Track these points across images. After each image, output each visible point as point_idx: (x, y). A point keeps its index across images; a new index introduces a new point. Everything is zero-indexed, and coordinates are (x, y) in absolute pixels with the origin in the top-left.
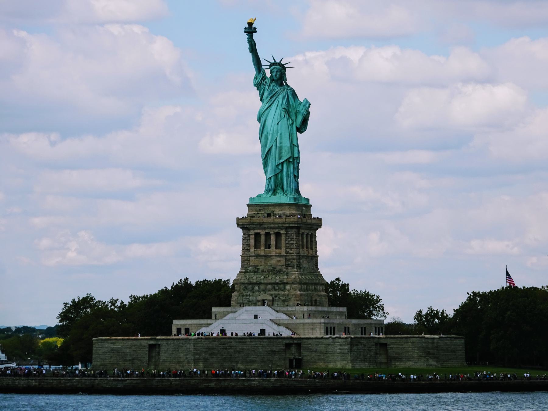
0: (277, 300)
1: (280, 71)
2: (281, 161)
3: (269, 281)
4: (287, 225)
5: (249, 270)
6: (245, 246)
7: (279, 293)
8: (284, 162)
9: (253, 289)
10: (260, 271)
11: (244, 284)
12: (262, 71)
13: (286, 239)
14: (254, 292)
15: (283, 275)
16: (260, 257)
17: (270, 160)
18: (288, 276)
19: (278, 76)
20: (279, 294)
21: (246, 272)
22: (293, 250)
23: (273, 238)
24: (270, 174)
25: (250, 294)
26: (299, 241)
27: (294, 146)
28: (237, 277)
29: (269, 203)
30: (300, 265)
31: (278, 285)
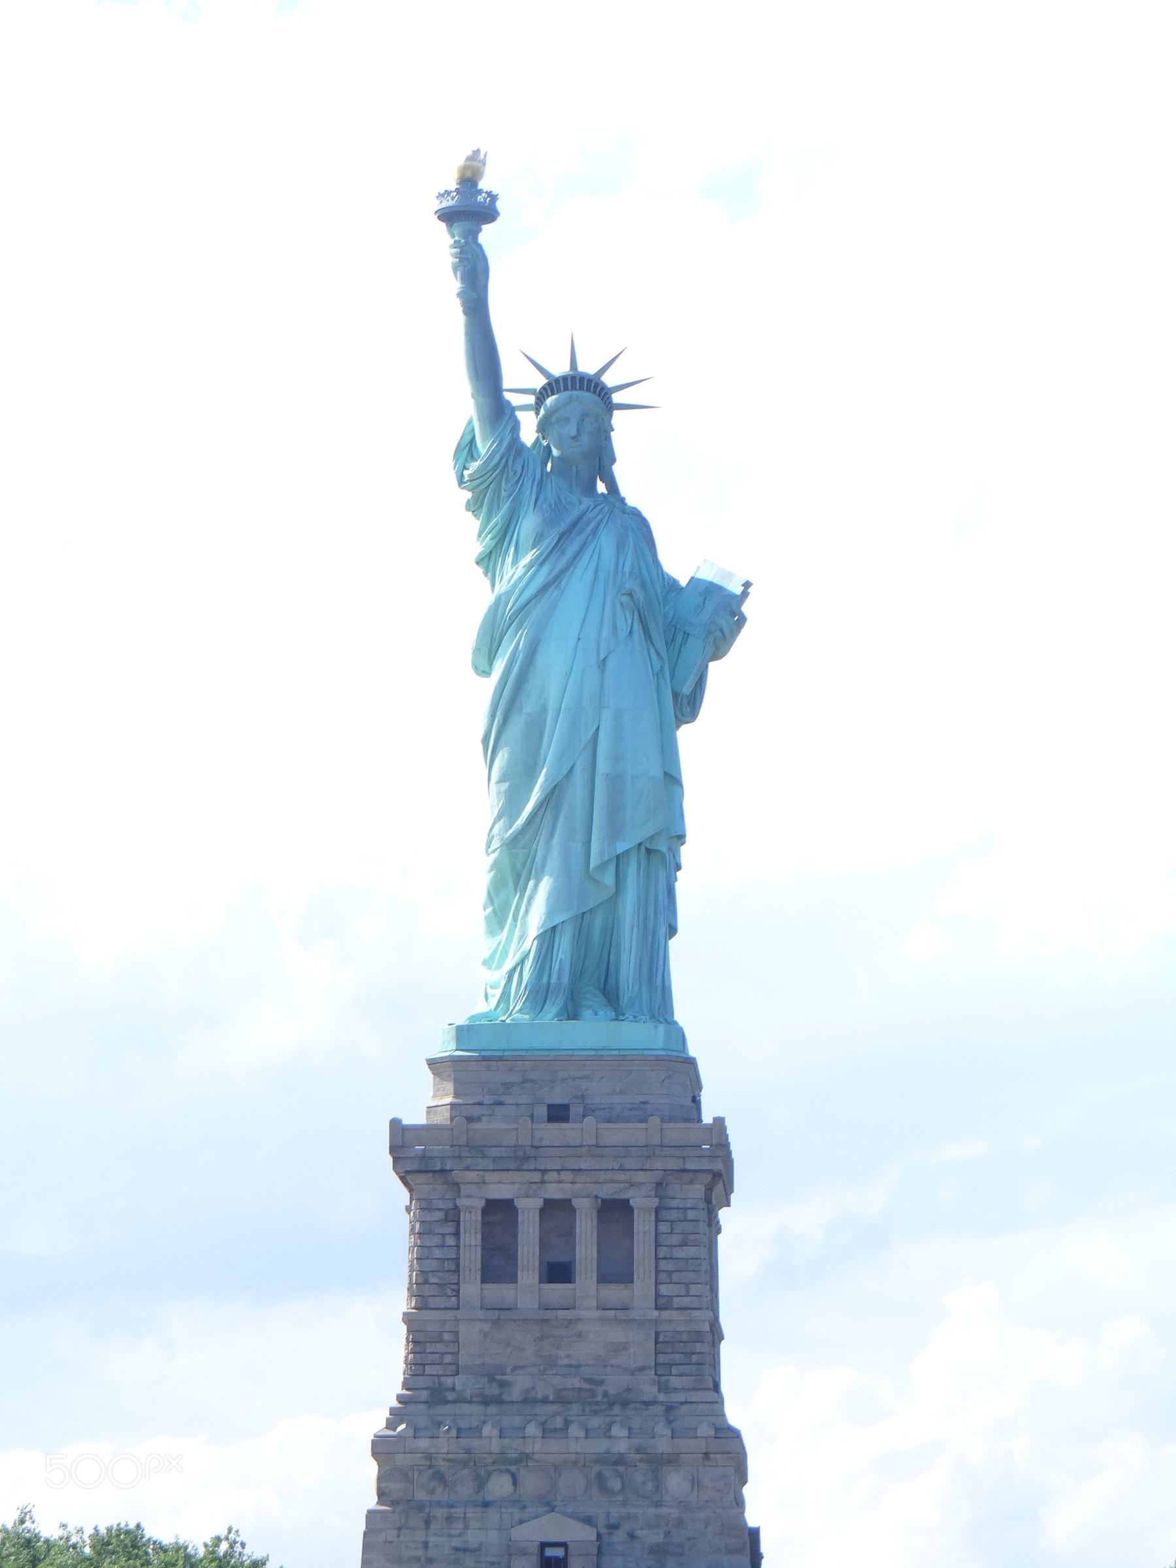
2: (621, 847)
4: (672, 1164)
5: (453, 1389)
8: (628, 851)
10: (516, 1394)
12: (508, 412)
14: (486, 1505)
19: (585, 439)
20: (629, 1517)
22: (694, 1289)
23: (586, 1227)
28: (391, 1425)
29: (553, 1053)
31: (621, 1469)
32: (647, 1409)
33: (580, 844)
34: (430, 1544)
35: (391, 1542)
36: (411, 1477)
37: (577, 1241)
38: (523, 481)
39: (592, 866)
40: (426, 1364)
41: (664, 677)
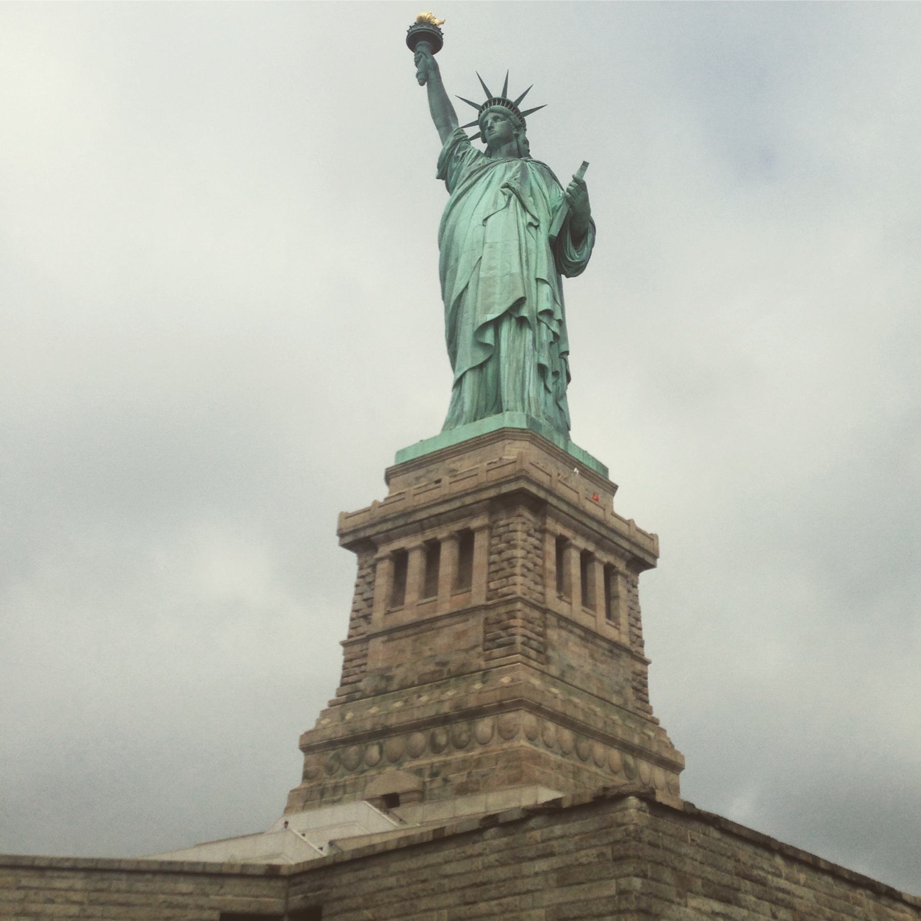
0: (436, 792)
1: (506, 116)
2: (490, 317)
3: (418, 714)
4: (492, 493)
7: (449, 758)
10: (395, 685)
11: (332, 744)
13: (490, 545)
14: (363, 772)
18: (487, 681)
20: (446, 764)
22: (511, 580)
26: (543, 558)
27: (539, 283)
30: (546, 649)
31: (448, 727)
41: (540, 231)
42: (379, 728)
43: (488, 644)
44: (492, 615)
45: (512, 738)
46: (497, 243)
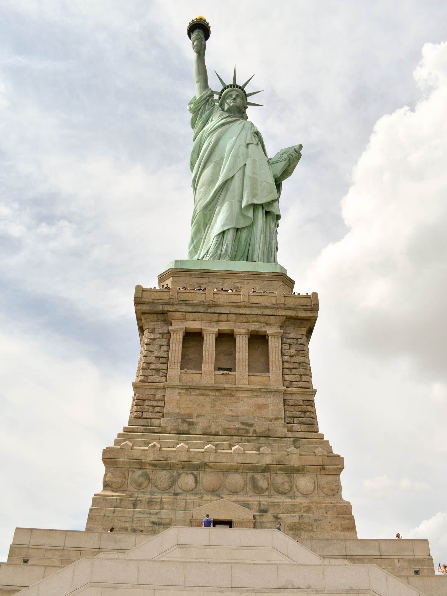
2: (256, 202)
3: (237, 459)
4: (290, 313)
6: (152, 359)
9: (173, 484)
10: (198, 429)
11: (141, 464)
14: (176, 494)
15: (282, 447)
16: (198, 392)
17: (226, 200)
20: (274, 505)
21: (149, 430)
22: (304, 378)
24: (224, 225)
25: (164, 500)
28: (117, 442)
31: (267, 475)
32: (281, 440)
33: (237, 201)
34: (135, 519)
35: (108, 516)
36: (127, 476)
37: (237, 350)
38: (214, 108)
39: (243, 206)
40: (144, 412)
42: (196, 462)
43: (289, 419)
44: (288, 398)
45: (333, 495)
46: (256, 161)
